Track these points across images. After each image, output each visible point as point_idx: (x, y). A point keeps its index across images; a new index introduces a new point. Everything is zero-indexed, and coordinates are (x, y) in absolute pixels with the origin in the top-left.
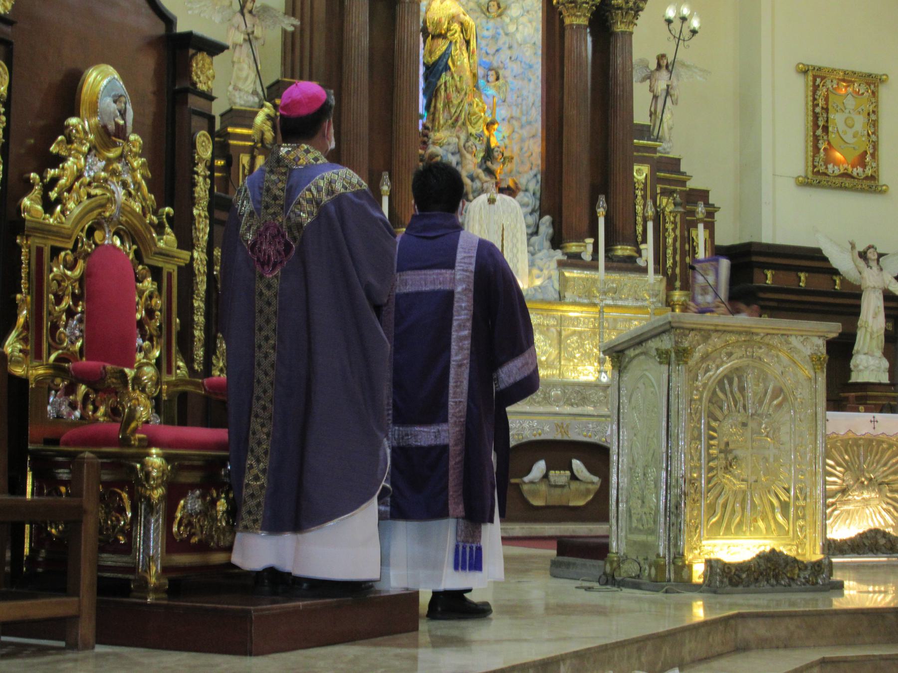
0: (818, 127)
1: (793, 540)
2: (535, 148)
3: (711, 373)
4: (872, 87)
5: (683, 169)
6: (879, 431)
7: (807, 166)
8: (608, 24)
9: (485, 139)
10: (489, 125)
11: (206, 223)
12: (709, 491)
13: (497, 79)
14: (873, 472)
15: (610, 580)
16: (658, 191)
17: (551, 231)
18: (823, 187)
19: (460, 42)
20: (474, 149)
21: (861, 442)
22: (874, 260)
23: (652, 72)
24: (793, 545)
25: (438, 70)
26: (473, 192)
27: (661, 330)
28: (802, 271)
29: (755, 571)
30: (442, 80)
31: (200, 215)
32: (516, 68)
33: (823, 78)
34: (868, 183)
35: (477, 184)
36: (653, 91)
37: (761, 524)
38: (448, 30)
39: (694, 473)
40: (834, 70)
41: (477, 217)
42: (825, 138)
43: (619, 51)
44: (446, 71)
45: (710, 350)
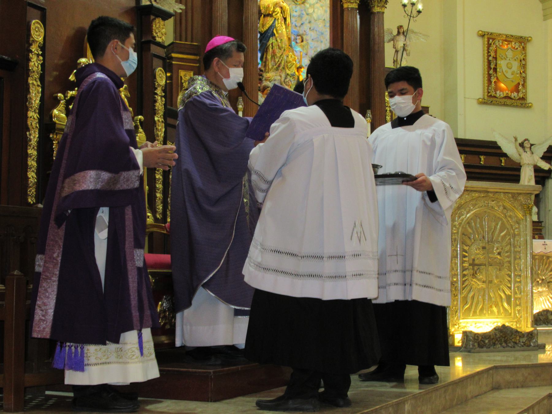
0: (491, 68)
1: (514, 319)
3: (464, 217)
4: (523, 44)
7: (484, 92)
8: (369, 7)
9: (296, 77)
11: (162, 125)
12: (463, 289)
13: (302, 41)
14: (544, 275)
18: (494, 104)
19: (281, 19)
20: (290, 84)
21: (536, 257)
22: (528, 148)
23: (394, 36)
24: (514, 322)
25: (268, 35)
28: (482, 155)
29: (493, 339)
30: (270, 42)
31: (159, 121)
33: (493, 39)
34: (521, 102)
36: (395, 48)
37: (495, 309)
38: (274, 11)
39: (455, 278)
40: (500, 35)
42: (495, 75)
43: (376, 23)
44: (272, 36)
45: (463, 202)
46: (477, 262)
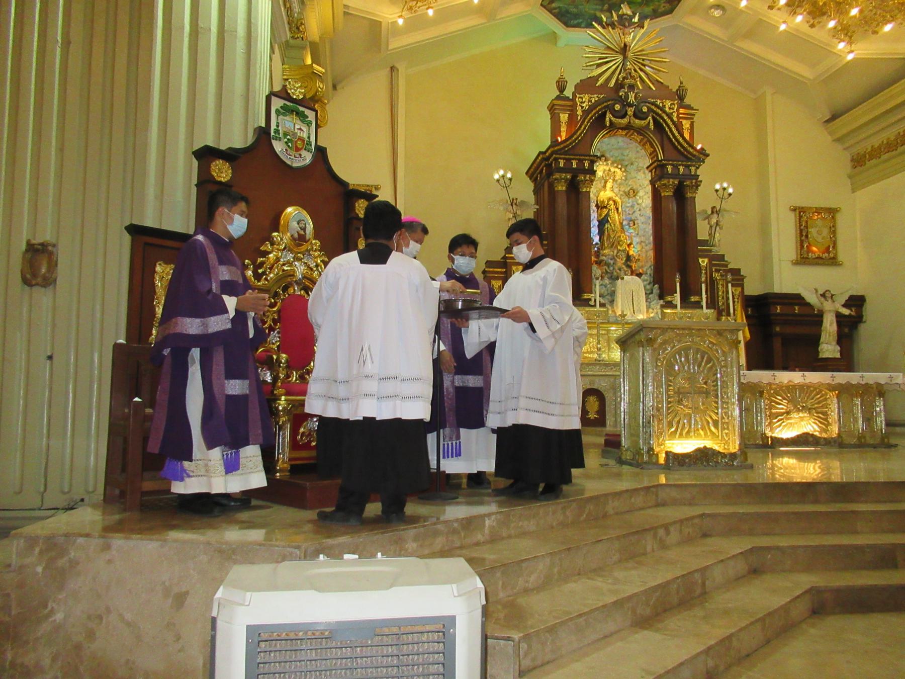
0: (803, 235)
1: (721, 441)
2: (651, 254)
5: (726, 259)
6: (808, 381)
10: (629, 245)
13: (634, 225)
15: (621, 462)
16: (714, 270)
17: (658, 291)
21: (797, 387)
27: (639, 329)
28: (796, 305)
32: (642, 219)
34: (831, 261)
37: (702, 432)
38: (608, 204)
40: (810, 208)
46: (682, 390)
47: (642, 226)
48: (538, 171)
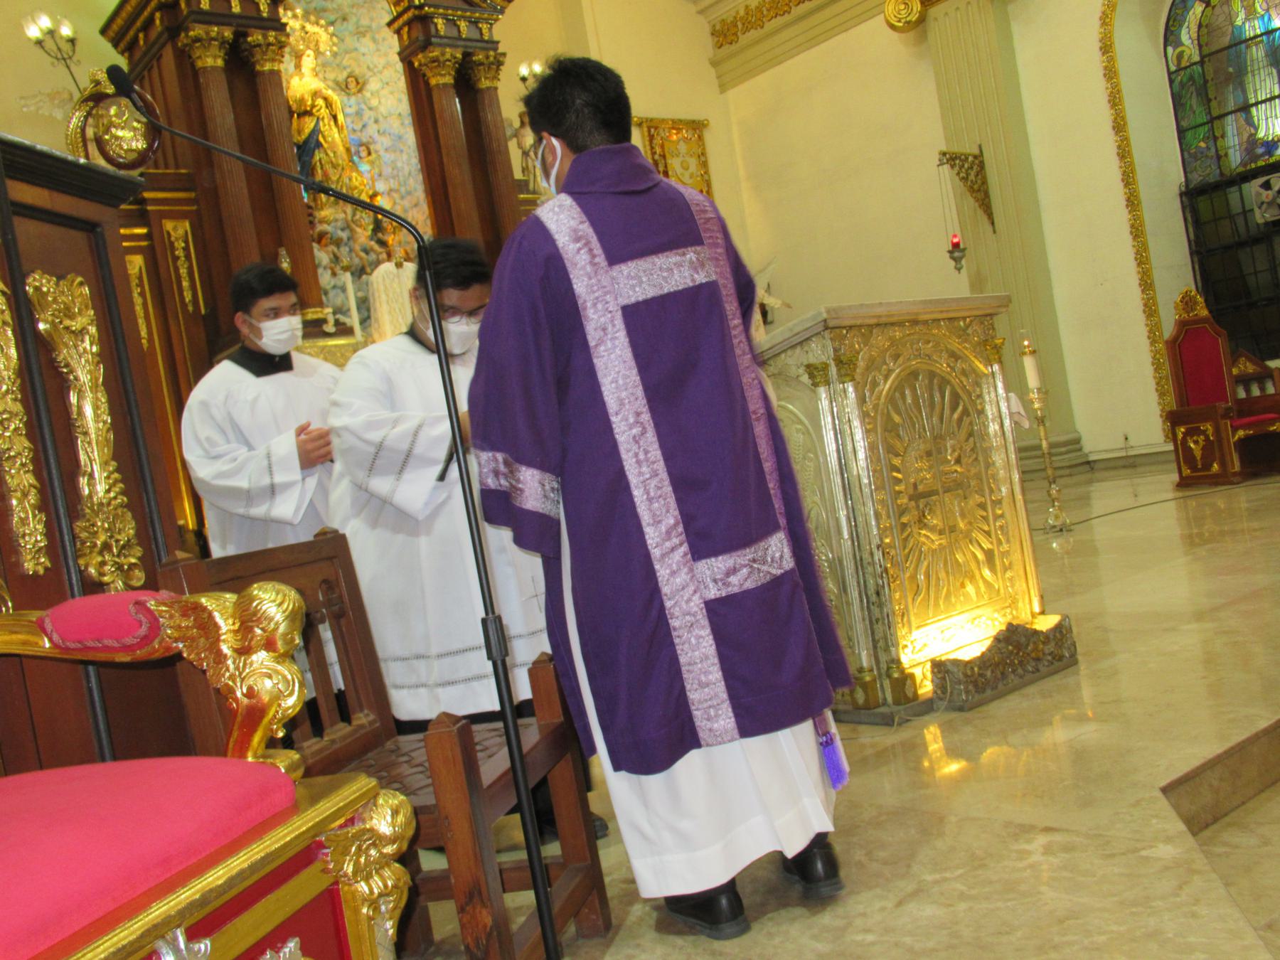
13: (369, 154)
23: (516, 130)
26: (371, 264)
30: (317, 157)
33: (656, 128)
35: (373, 257)
38: (313, 106)
39: (886, 537)
40: (663, 121)
41: (382, 288)
47: (387, 157)
48: (139, 24)
